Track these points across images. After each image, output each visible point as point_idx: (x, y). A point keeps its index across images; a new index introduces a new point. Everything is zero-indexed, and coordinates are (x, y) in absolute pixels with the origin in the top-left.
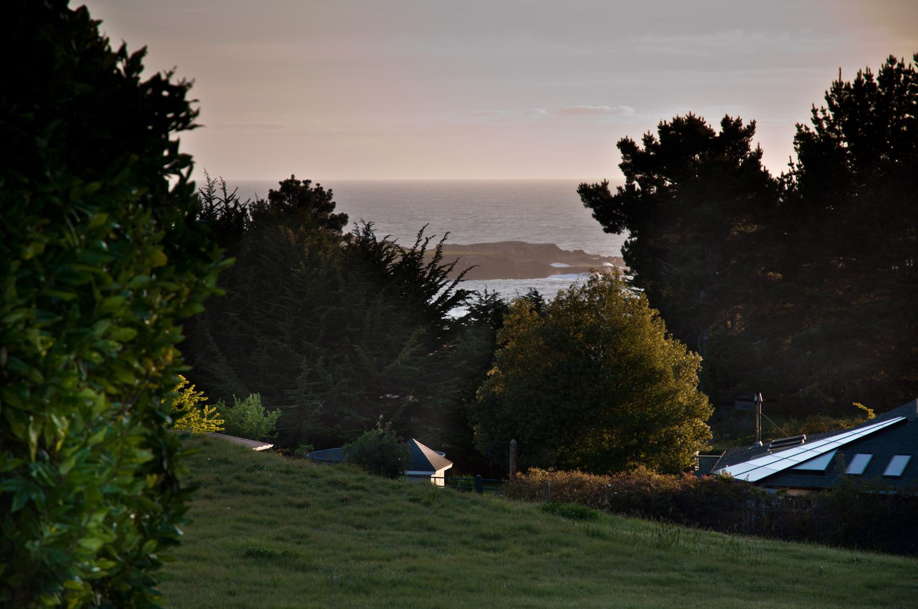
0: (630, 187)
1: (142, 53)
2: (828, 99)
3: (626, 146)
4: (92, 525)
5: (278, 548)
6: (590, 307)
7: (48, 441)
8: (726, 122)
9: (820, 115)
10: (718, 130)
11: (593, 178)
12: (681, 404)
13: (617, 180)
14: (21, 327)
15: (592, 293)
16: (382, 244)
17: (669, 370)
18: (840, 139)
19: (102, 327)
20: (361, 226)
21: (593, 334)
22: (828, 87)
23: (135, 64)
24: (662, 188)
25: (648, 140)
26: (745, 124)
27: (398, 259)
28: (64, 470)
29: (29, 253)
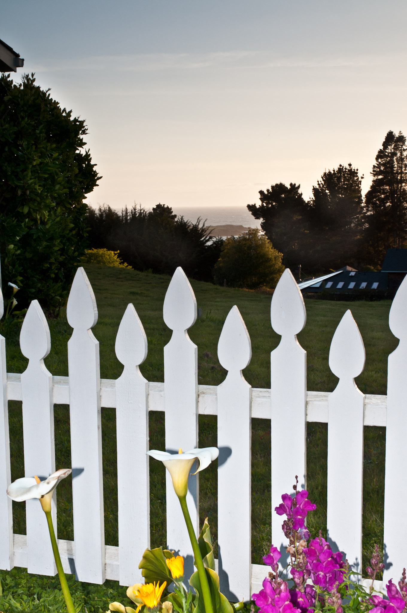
0: (263, 205)
1: (71, 112)
2: (322, 177)
3: (261, 192)
4: (56, 243)
5: (139, 292)
6: (249, 239)
7: (43, 219)
8: (291, 184)
9: (320, 183)
10: (289, 187)
11: (251, 203)
12: (276, 269)
13: (258, 204)
14: (33, 185)
15: (250, 234)
16: (186, 222)
17: (273, 258)
18: (326, 190)
19: (57, 187)
20: (180, 217)
21: (250, 248)
22: (322, 174)
23: (69, 115)
24: (272, 205)
25: (268, 190)
26: (297, 186)
27: (191, 227)
28: (47, 227)
29: (35, 163)
